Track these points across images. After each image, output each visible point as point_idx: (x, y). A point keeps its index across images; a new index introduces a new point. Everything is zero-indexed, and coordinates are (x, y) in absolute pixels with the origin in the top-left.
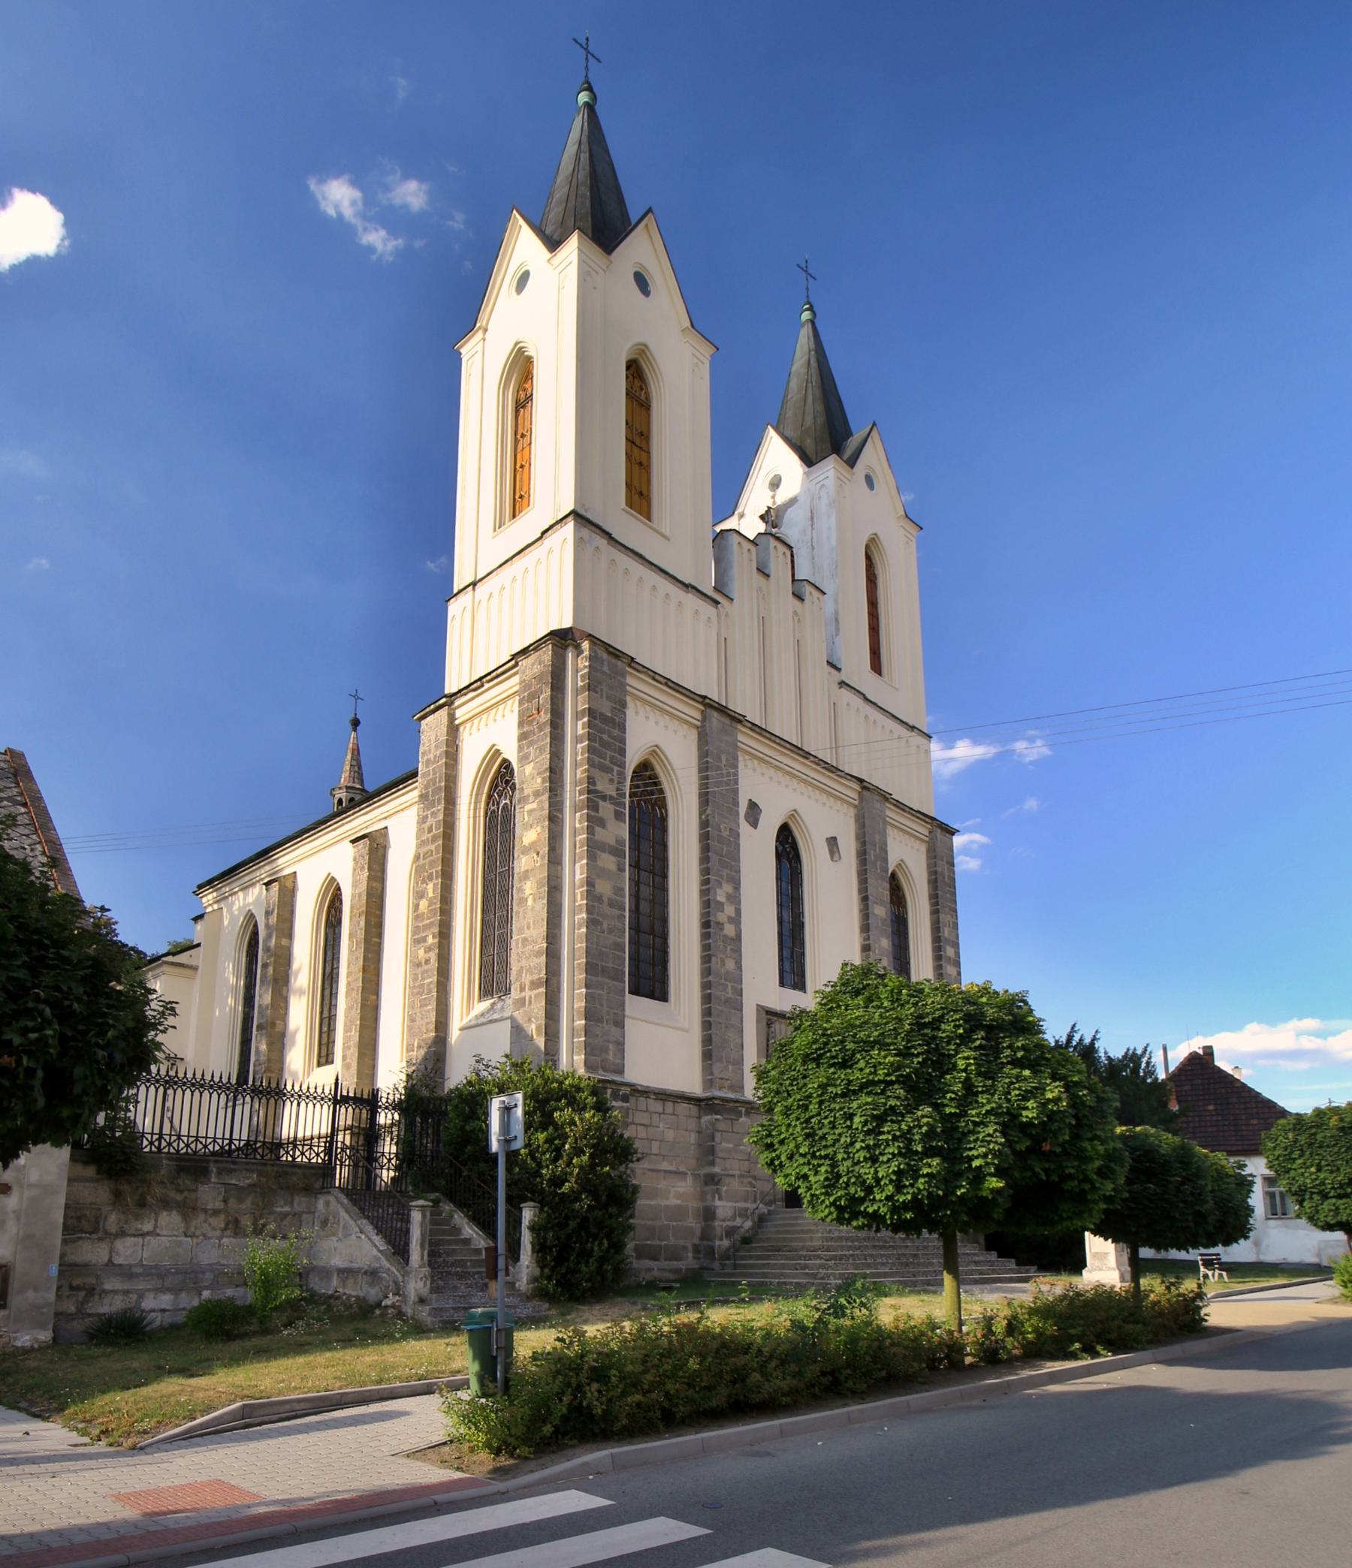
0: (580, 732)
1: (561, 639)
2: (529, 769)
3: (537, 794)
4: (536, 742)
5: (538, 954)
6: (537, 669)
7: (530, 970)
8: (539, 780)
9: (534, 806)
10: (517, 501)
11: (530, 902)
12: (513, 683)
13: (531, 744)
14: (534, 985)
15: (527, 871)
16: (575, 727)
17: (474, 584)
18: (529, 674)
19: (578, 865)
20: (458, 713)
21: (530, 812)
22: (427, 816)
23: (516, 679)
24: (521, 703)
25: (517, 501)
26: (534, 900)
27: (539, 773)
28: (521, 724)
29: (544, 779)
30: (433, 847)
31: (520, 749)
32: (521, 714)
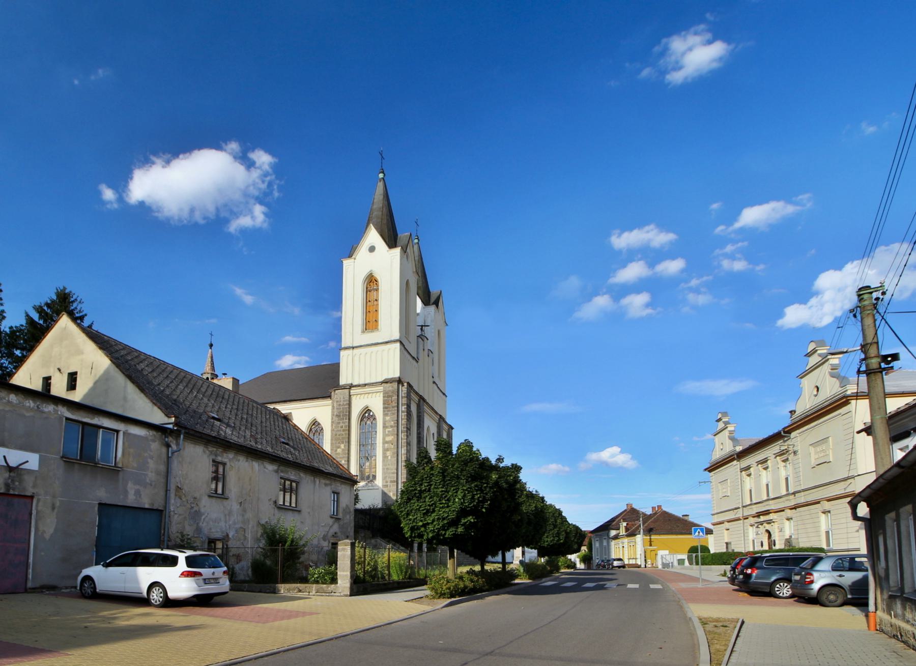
0: (403, 409)
1: (399, 381)
2: (388, 418)
3: (392, 427)
4: (392, 411)
5: (393, 473)
6: (391, 389)
7: (390, 477)
8: (392, 423)
9: (391, 429)
10: (370, 322)
11: (389, 458)
12: (381, 388)
13: (389, 411)
14: (391, 482)
15: (388, 449)
16: (403, 408)
17: (353, 348)
18: (387, 389)
19: (403, 449)
20: (351, 391)
21: (389, 431)
22: (340, 423)
23: (382, 388)
24: (384, 397)
25: (370, 322)
26: (391, 457)
27: (393, 421)
28: (384, 404)
29: (395, 423)
30: (343, 433)
31: (384, 411)
32: (384, 401)
